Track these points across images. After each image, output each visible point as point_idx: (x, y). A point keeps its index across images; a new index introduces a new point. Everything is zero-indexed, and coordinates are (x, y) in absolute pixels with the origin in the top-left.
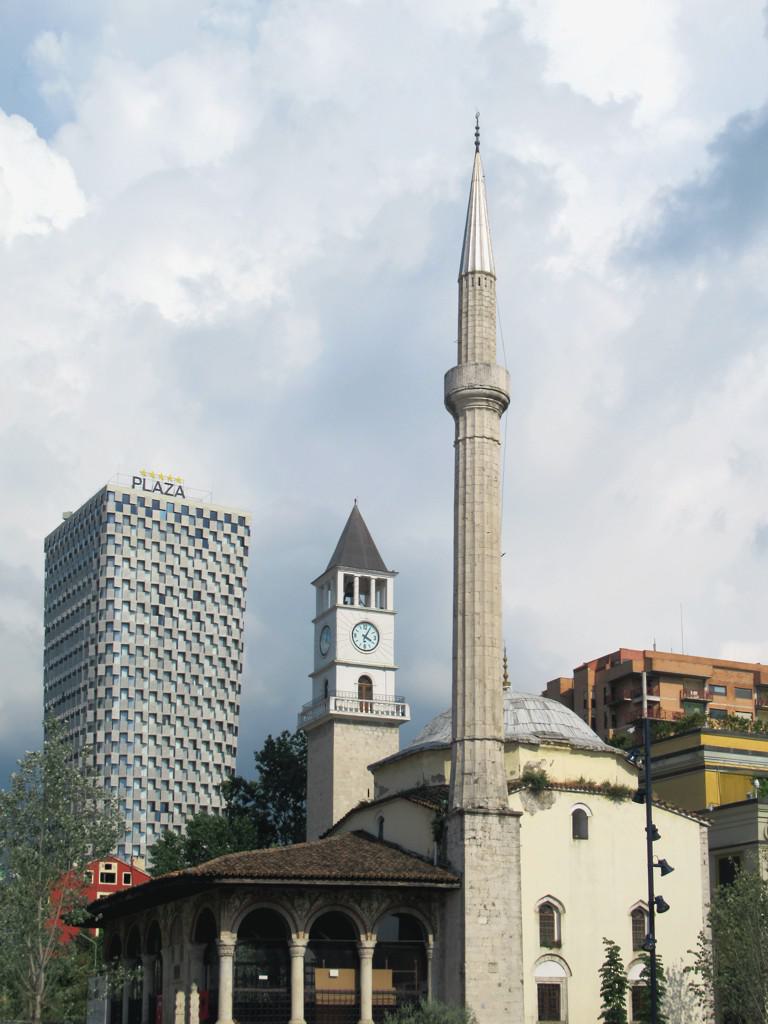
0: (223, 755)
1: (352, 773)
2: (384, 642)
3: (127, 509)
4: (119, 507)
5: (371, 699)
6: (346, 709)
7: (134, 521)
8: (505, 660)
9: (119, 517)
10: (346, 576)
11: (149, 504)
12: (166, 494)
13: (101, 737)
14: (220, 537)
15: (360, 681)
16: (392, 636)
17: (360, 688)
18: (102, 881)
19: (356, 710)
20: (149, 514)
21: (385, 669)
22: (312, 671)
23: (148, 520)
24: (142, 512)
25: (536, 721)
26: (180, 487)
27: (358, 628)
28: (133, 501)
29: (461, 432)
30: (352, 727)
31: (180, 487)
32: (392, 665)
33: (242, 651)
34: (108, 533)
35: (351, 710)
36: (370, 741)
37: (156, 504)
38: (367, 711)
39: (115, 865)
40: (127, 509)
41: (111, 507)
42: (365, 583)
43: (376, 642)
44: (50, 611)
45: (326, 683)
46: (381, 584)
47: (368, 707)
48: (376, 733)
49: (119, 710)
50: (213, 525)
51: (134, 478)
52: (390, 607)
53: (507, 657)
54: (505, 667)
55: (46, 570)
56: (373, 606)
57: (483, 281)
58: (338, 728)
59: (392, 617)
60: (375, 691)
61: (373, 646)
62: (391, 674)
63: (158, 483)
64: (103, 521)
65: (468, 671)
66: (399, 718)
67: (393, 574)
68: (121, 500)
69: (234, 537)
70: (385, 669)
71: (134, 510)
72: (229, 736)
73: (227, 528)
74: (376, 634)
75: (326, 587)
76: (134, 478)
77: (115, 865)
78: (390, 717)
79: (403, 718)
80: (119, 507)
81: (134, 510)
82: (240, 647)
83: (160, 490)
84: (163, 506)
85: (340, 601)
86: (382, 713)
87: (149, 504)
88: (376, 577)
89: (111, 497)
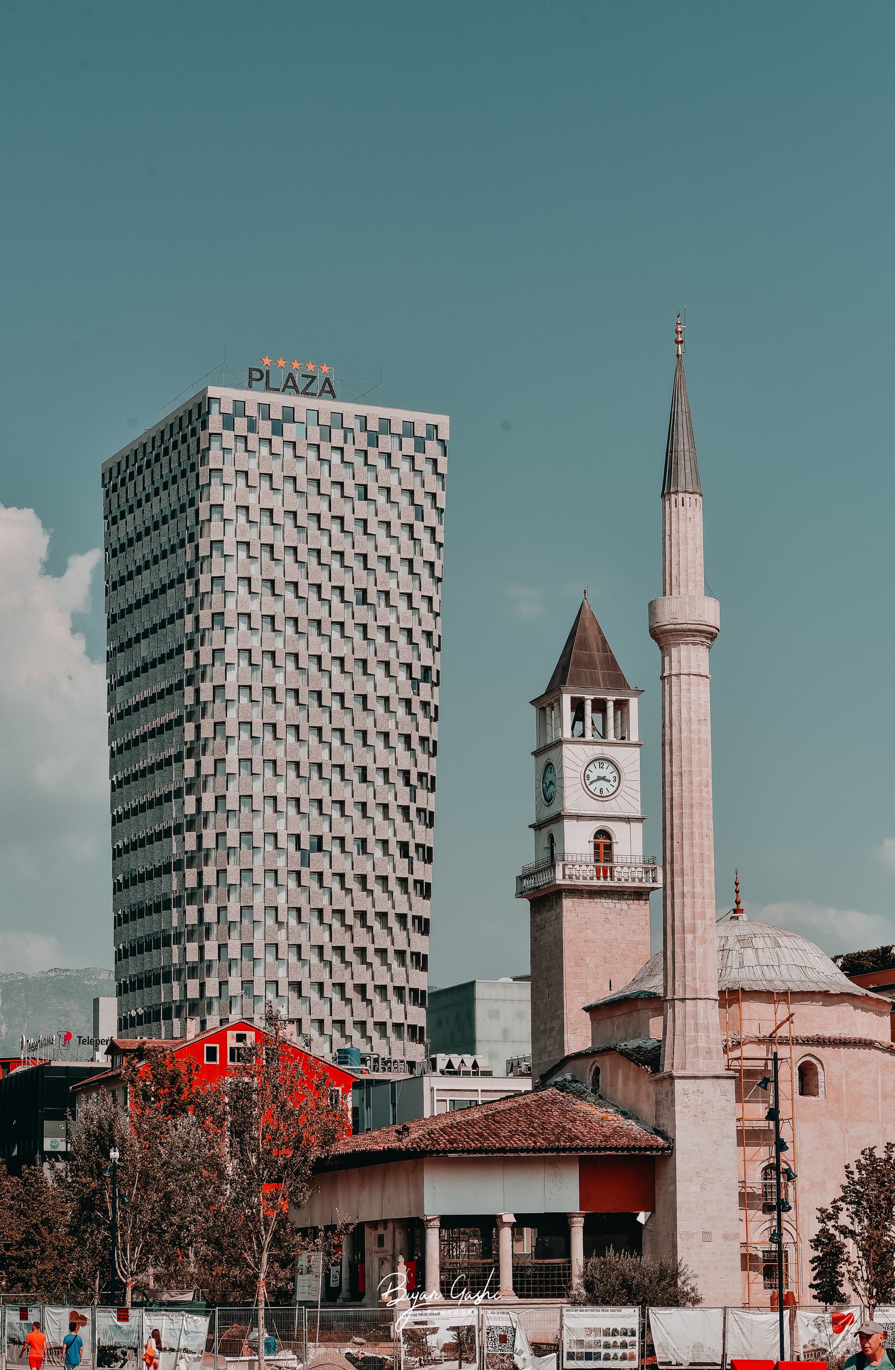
0: (411, 863)
1: (588, 960)
2: (625, 789)
3: (241, 425)
4: (228, 422)
5: (611, 861)
6: (578, 878)
7: (253, 444)
8: (737, 884)
9: (228, 438)
10: (573, 700)
11: (277, 414)
12: (305, 393)
13: (208, 804)
14: (397, 460)
15: (595, 837)
16: (637, 776)
17: (597, 847)
18: (232, 1060)
19: (592, 878)
20: (278, 429)
21: (628, 820)
22: (533, 821)
23: (277, 441)
24: (265, 428)
25: (763, 962)
26: (327, 380)
27: (591, 767)
28: (252, 411)
29: (667, 667)
30: (586, 901)
31: (327, 380)
32: (639, 815)
33: (436, 719)
34: (211, 466)
35: (585, 878)
36: (609, 917)
37: (289, 415)
38: (605, 878)
39: (251, 1036)
40: (241, 425)
41: (215, 423)
42: (600, 706)
43: (616, 784)
44: (114, 588)
45: (551, 838)
46: (621, 705)
47: (607, 873)
48: (618, 906)
49: (236, 758)
50: (387, 443)
51: (251, 370)
52: (634, 737)
53: (739, 880)
54: (737, 892)
55: (106, 518)
56: (611, 737)
57: (687, 500)
58: (567, 903)
59: (638, 750)
60: (616, 849)
61: (612, 790)
62: (637, 827)
63: (291, 376)
64: (202, 446)
65: (677, 923)
66: (648, 885)
67: (638, 692)
68: (230, 411)
69: (420, 458)
70: (628, 820)
71: (252, 426)
72: (421, 793)
73: (409, 444)
74: (615, 774)
75: (548, 709)
76: (251, 370)
77: (251, 1036)
78: (636, 884)
79: (655, 885)
80: (228, 422)
81: (252, 426)
82: (436, 644)
83: (295, 387)
84: (300, 416)
85: (567, 734)
86: (626, 880)
87: (277, 414)
88: (614, 698)
89: (215, 407)
